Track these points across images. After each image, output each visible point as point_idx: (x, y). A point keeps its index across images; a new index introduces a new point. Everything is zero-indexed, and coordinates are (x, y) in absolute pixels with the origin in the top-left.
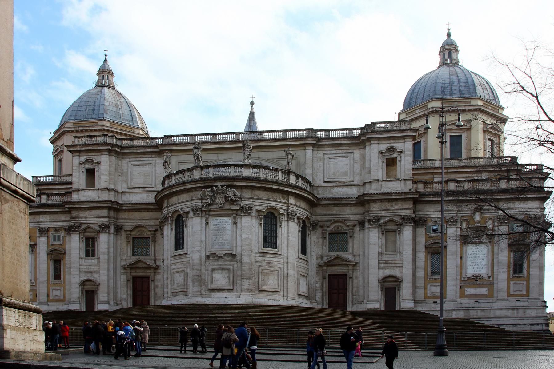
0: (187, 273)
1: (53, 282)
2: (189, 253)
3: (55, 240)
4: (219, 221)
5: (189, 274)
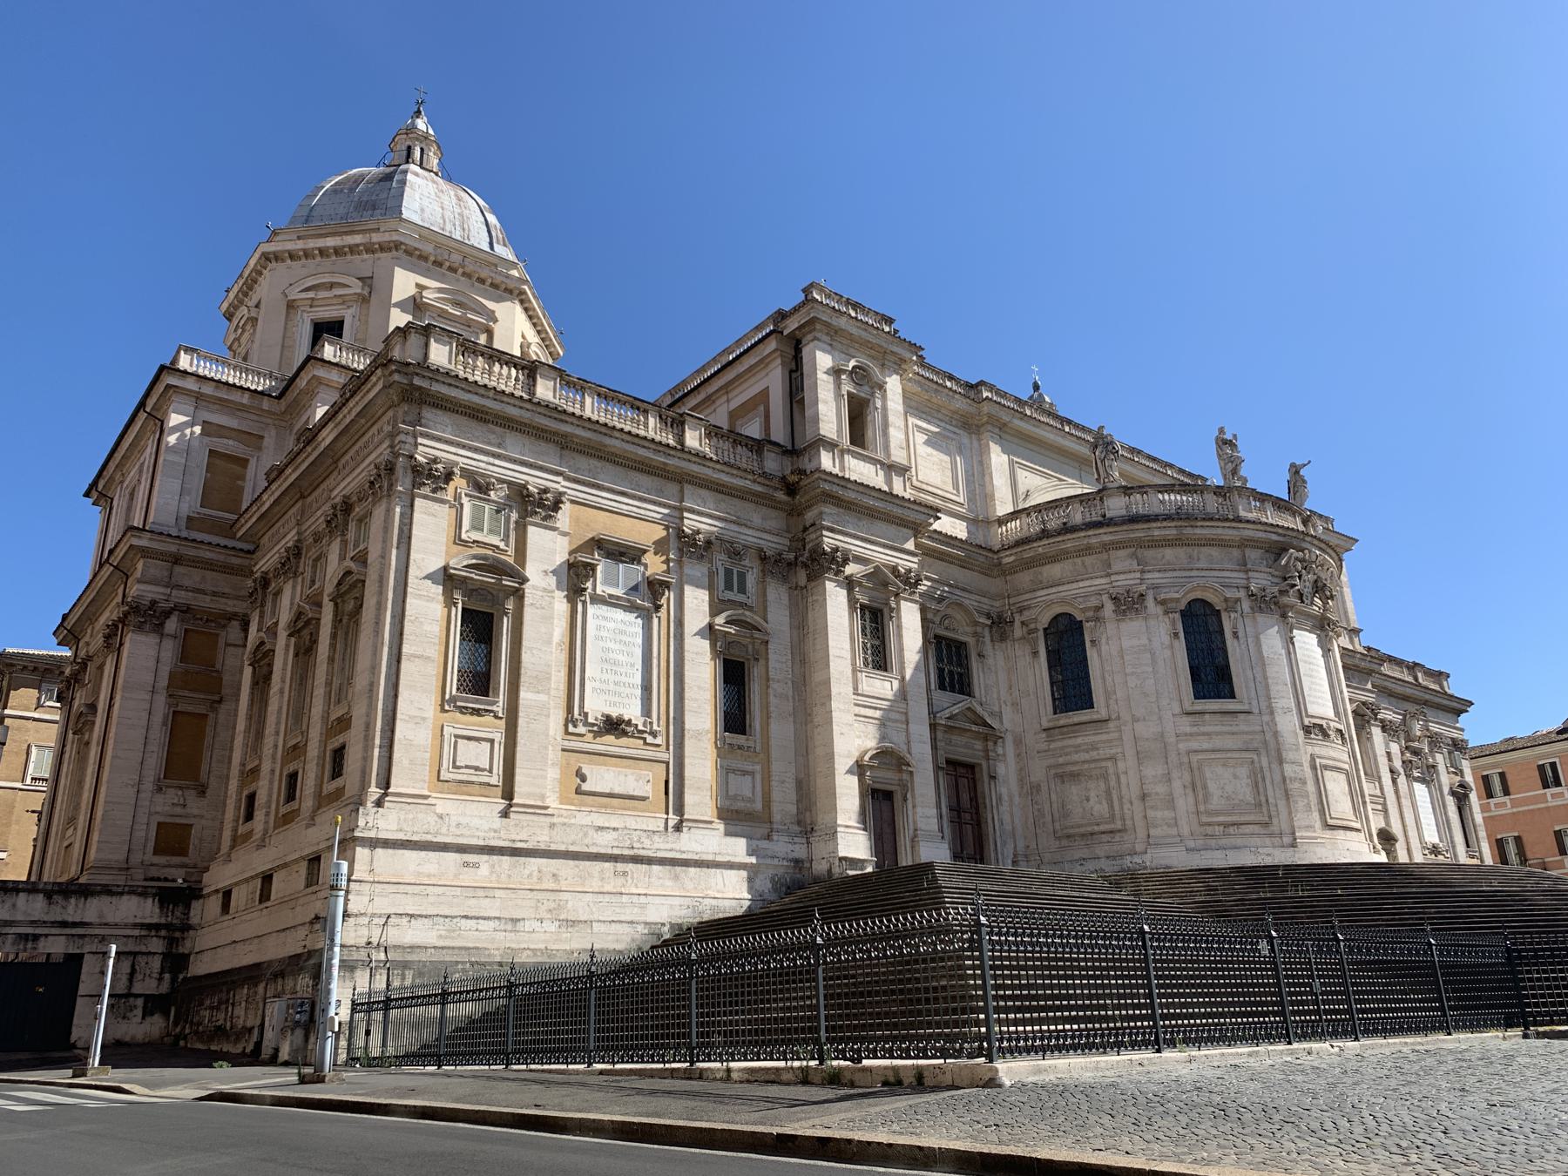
0: (1261, 768)
1: (728, 741)
2: (1256, 711)
3: (729, 586)
4: (1306, 640)
5: (1267, 774)
